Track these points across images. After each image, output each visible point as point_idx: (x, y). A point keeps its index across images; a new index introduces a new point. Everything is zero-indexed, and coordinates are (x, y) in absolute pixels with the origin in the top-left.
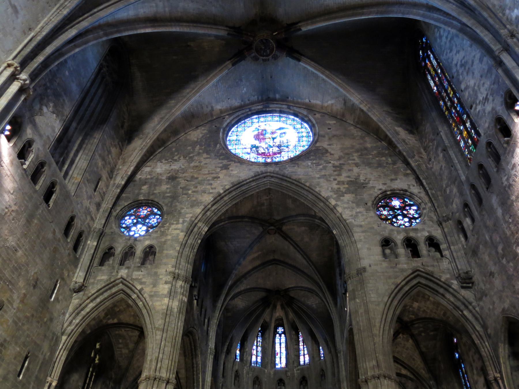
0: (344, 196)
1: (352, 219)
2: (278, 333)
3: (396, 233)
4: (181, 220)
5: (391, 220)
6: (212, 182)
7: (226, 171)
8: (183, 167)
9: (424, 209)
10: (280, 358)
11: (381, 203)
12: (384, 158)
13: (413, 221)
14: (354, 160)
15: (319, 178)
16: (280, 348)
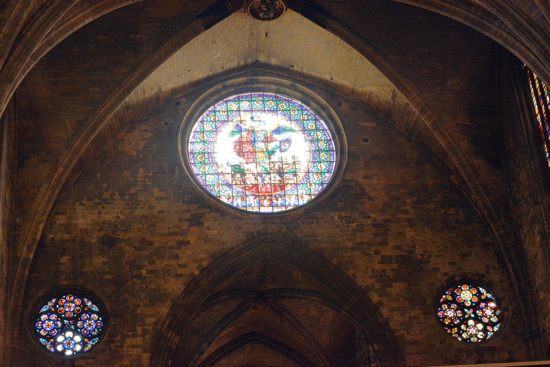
0: (391, 286)
1: (404, 329)
3: (464, 354)
4: (139, 329)
5: (458, 326)
6: (179, 252)
7: (198, 227)
8: (122, 217)
9: (506, 309)
11: (446, 295)
12: (452, 211)
13: (488, 328)
14: (406, 212)
15: (352, 249)
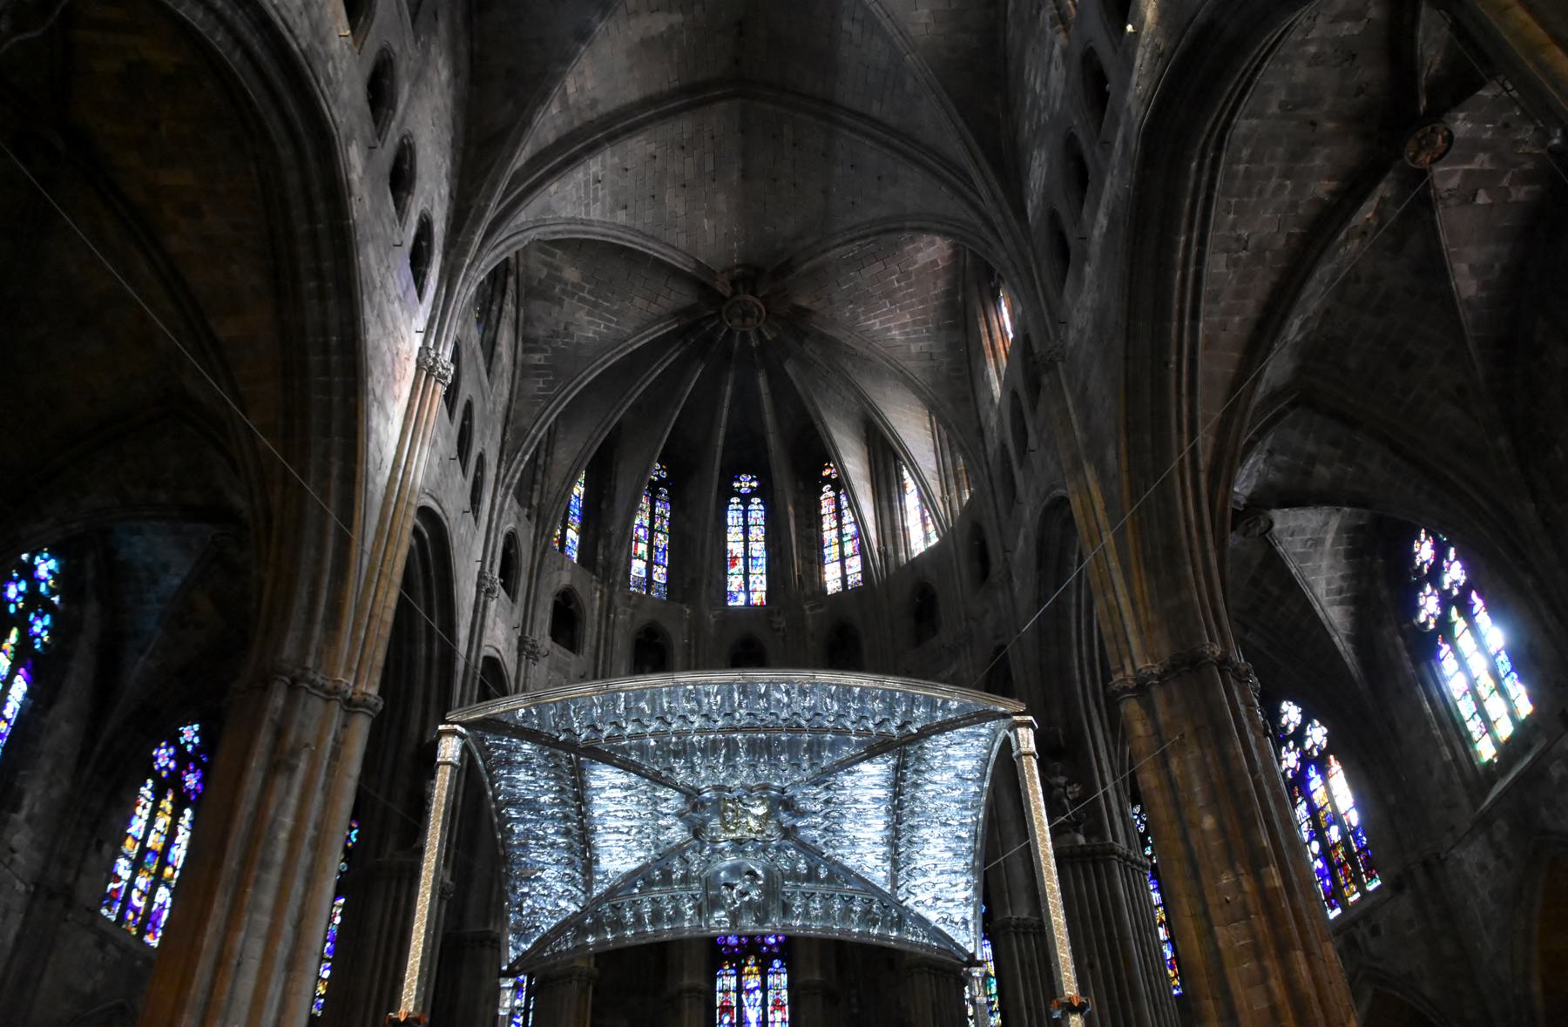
2: (738, 494)
10: (746, 575)
16: (746, 541)
